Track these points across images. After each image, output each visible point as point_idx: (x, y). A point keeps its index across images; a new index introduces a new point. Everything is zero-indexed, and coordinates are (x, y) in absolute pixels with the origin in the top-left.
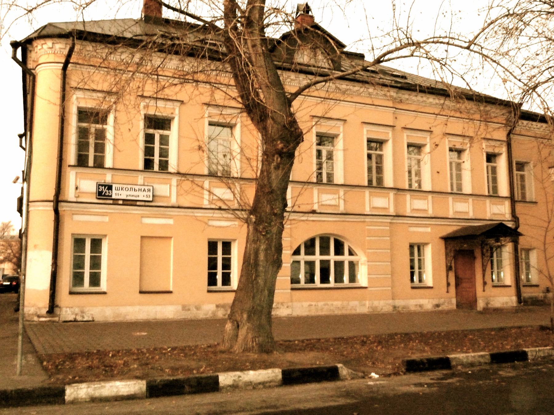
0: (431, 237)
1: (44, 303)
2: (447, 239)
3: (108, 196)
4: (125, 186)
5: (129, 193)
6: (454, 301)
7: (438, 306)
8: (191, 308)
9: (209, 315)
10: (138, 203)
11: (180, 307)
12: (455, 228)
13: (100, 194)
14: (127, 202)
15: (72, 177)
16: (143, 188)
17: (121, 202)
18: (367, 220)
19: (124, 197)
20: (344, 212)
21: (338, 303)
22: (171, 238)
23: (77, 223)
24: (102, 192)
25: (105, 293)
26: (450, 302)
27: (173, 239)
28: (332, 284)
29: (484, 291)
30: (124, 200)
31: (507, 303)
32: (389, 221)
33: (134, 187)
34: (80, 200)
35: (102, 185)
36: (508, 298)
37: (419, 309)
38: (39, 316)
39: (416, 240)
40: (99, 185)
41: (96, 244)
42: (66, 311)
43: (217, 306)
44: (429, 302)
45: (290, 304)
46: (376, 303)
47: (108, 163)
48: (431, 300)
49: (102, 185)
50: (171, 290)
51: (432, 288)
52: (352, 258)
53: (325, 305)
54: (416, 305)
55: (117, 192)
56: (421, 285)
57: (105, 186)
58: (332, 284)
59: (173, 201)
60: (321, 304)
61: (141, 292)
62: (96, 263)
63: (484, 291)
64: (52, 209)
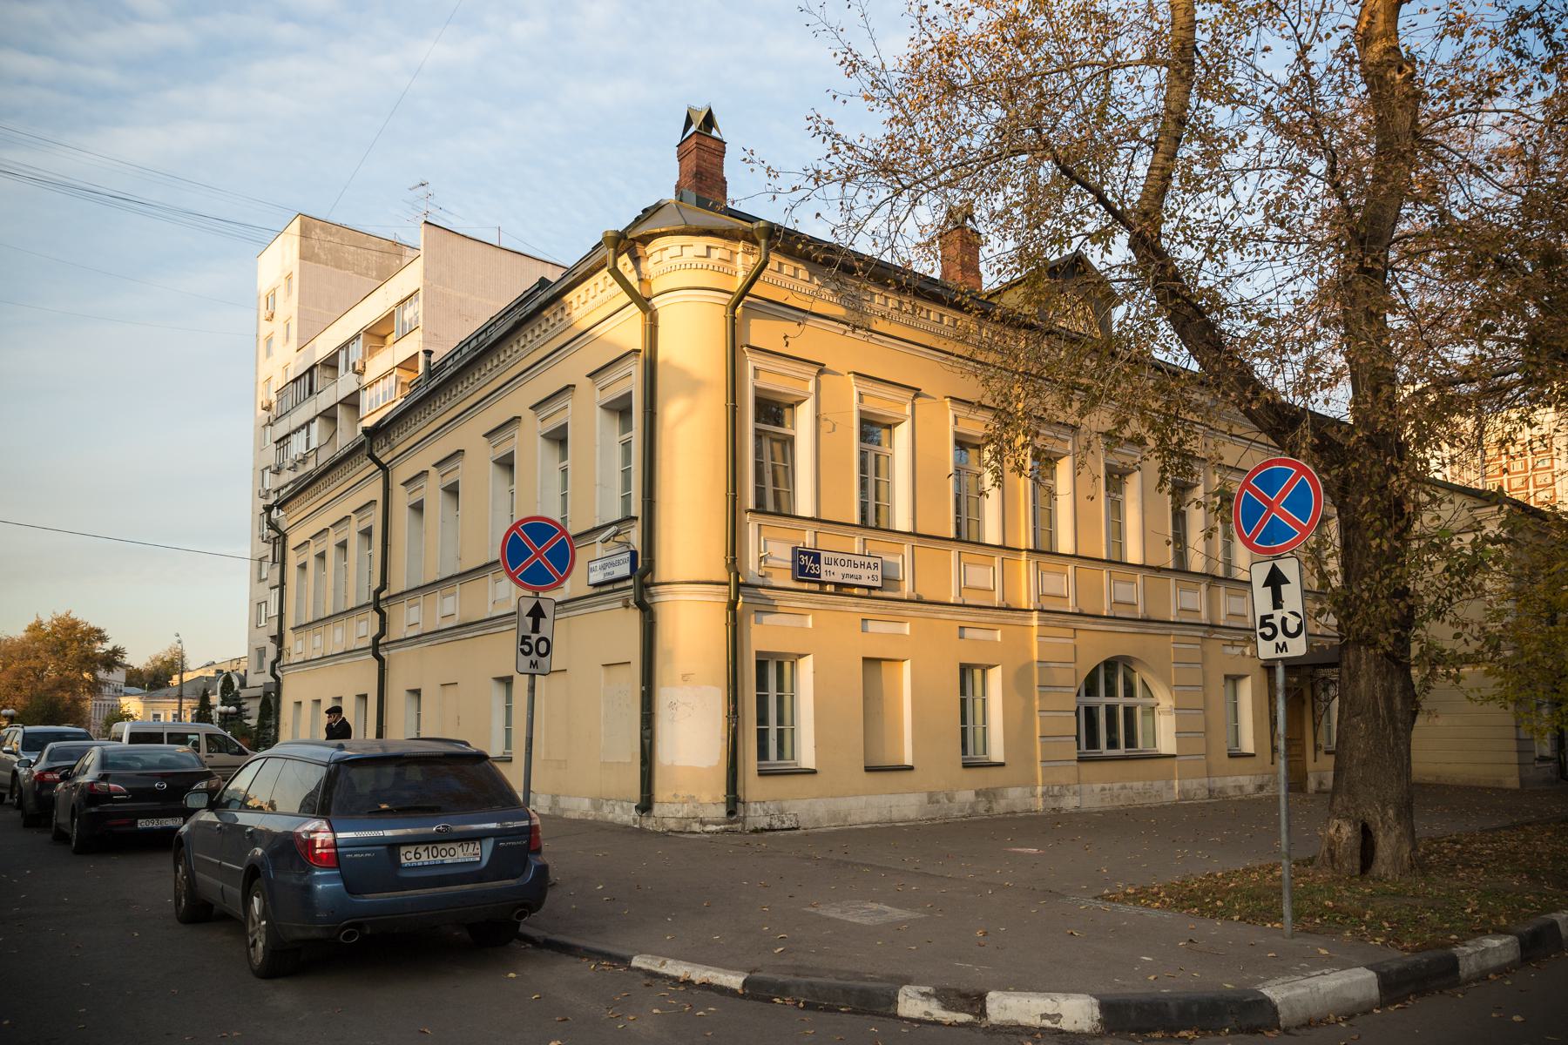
4: (840, 556)
10: (856, 591)
11: (925, 797)
16: (866, 560)
21: (1138, 785)
28: (1104, 749)
30: (837, 585)
35: (805, 553)
38: (702, 823)
40: (797, 553)
43: (977, 794)
45: (1077, 787)
49: (805, 553)
50: (908, 761)
53: (1124, 788)
55: (829, 568)
57: (809, 554)
58: (1104, 749)
60: (1117, 786)
61: (868, 769)
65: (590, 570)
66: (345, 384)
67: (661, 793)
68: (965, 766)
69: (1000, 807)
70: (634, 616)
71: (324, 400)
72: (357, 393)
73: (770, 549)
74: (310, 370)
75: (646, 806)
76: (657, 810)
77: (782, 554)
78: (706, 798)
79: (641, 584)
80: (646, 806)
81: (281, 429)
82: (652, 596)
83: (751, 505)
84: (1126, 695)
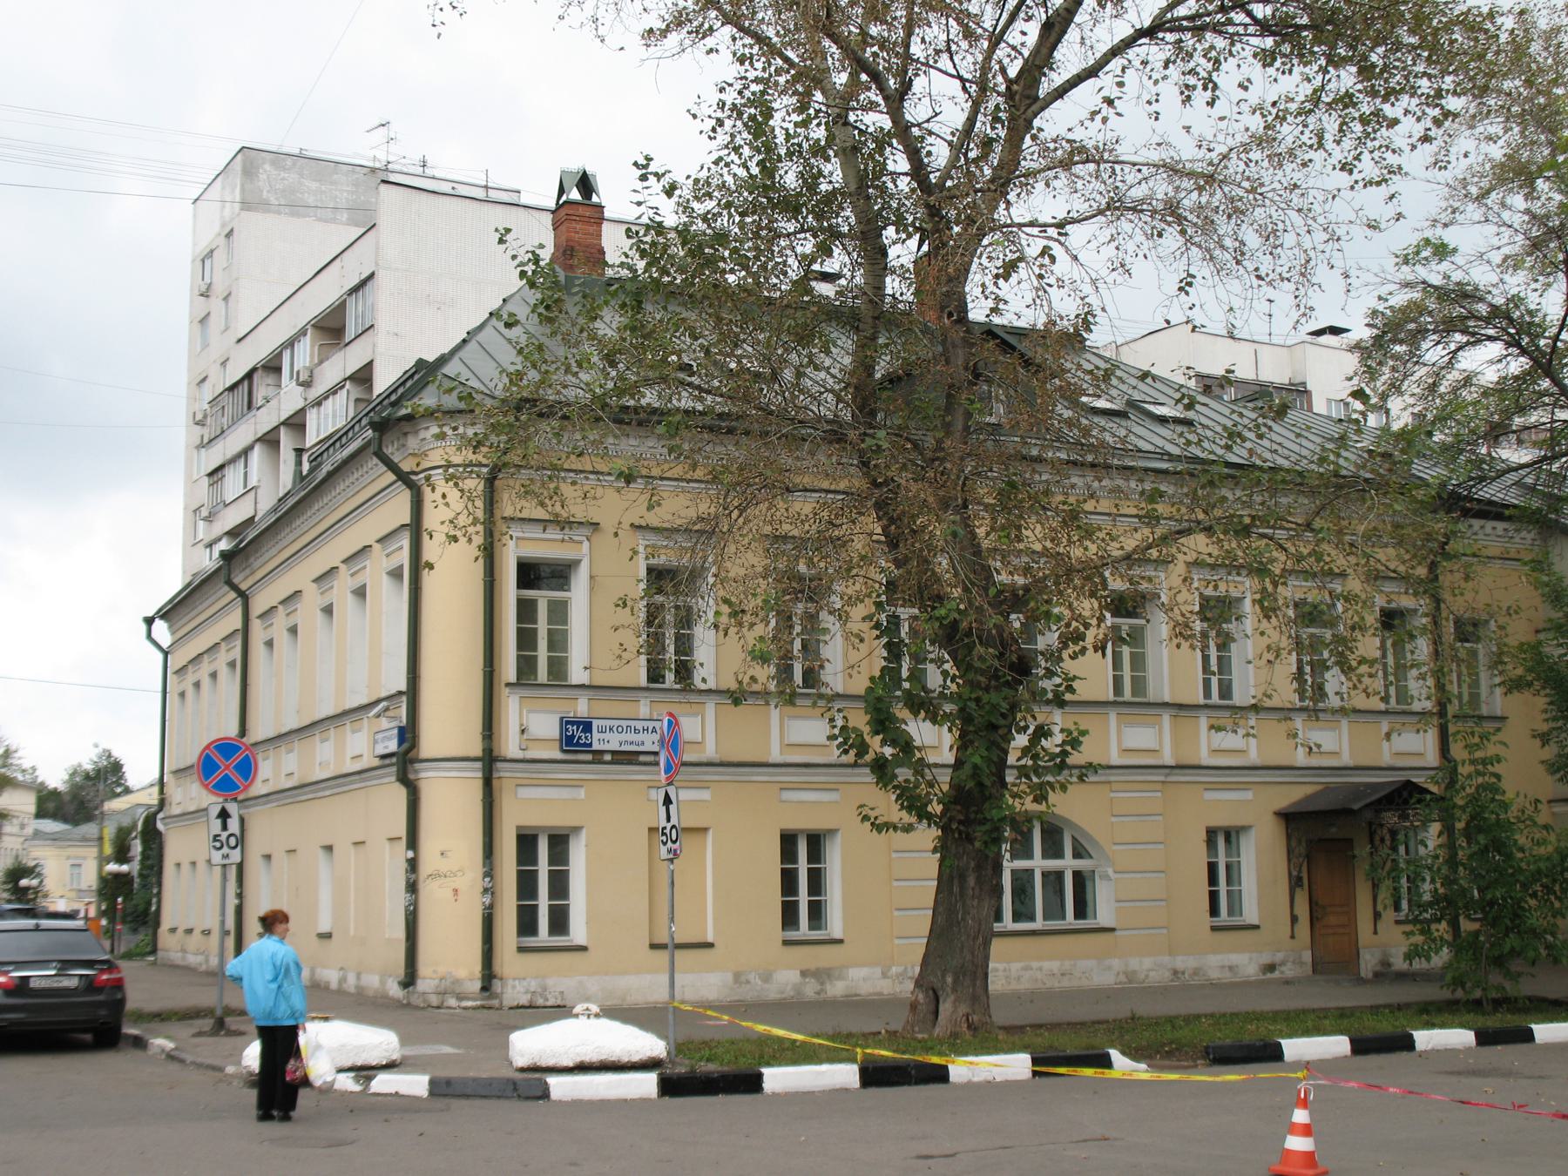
0: (1256, 811)
1: (468, 969)
2: (1290, 819)
3: (585, 745)
5: (624, 737)
6: (1307, 956)
7: (1271, 968)
8: (751, 977)
9: (789, 992)
10: (642, 758)
11: (730, 977)
12: (1310, 790)
14: (625, 758)
15: (512, 708)
17: (608, 757)
18: (1112, 778)
19: (614, 746)
21: (1054, 965)
22: (705, 830)
23: (526, 806)
24: (573, 736)
25: (583, 949)
26: (1295, 956)
27: (711, 832)
29: (1375, 932)
30: (613, 753)
32: (1162, 778)
33: (632, 723)
34: (530, 755)
35: (573, 723)
37: (1227, 977)
38: (460, 998)
39: (1221, 820)
40: (565, 723)
41: (559, 842)
42: (514, 987)
43: (804, 974)
46: (1134, 963)
47: (577, 675)
49: (573, 723)
50: (710, 939)
51: (1257, 927)
52: (1081, 864)
54: (1223, 967)
55: (602, 736)
56: (1236, 921)
57: (578, 724)
59: (710, 751)
61: (653, 946)
62: (560, 885)
63: (1375, 932)
64: (480, 775)
65: (375, 742)
66: (289, 398)
67: (424, 969)
68: (786, 943)
69: (836, 989)
70: (401, 793)
71: (265, 420)
72: (301, 412)
73: (530, 723)
74: (249, 376)
75: (409, 980)
76: (423, 985)
77: (546, 725)
78: (462, 973)
79: (405, 761)
80: (409, 980)
81: (215, 457)
82: (416, 772)
83: (512, 678)
84: (1045, 855)
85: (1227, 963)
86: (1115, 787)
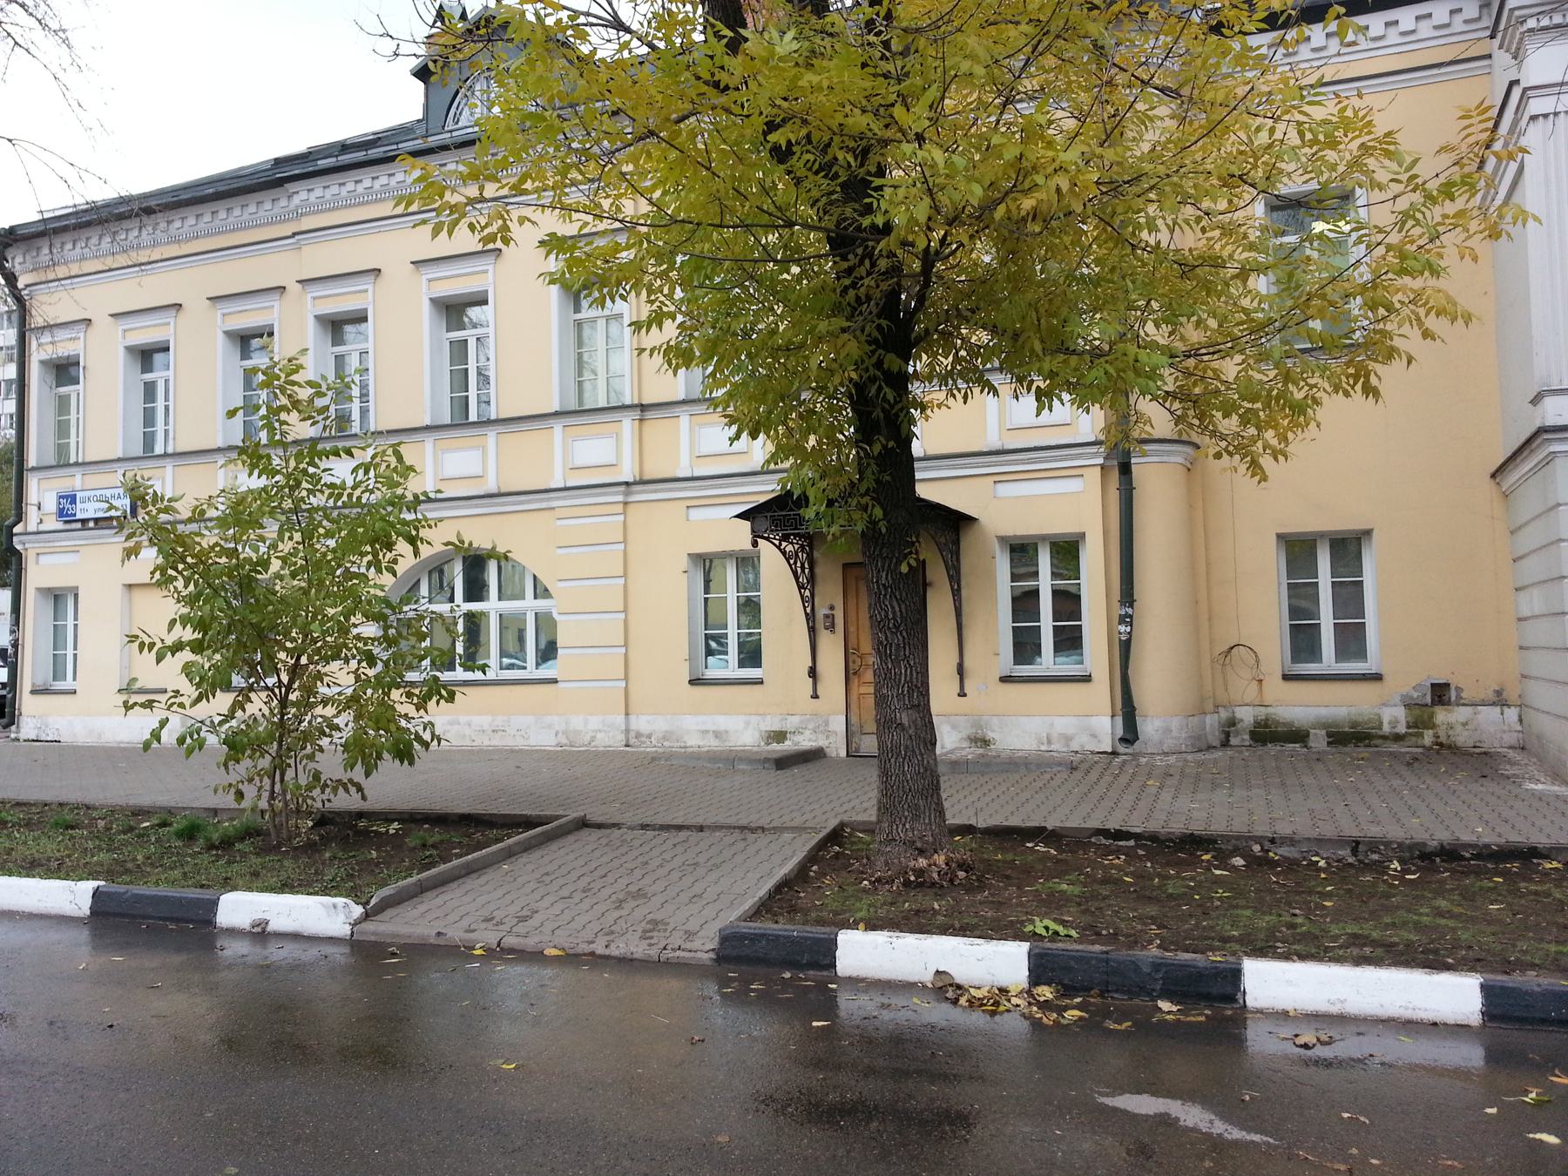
6: (838, 724)
13: (61, 513)
17: (91, 524)
20: (495, 491)
21: (484, 721)
29: (962, 694)
30: (96, 520)
31: (1068, 739)
32: (620, 498)
34: (42, 528)
36: (1073, 720)
37: (711, 743)
44: (747, 723)
46: (577, 722)
48: (754, 719)
53: (451, 723)
54: (705, 732)
57: (66, 497)
63: (962, 694)
85: (711, 727)
86: (558, 513)
